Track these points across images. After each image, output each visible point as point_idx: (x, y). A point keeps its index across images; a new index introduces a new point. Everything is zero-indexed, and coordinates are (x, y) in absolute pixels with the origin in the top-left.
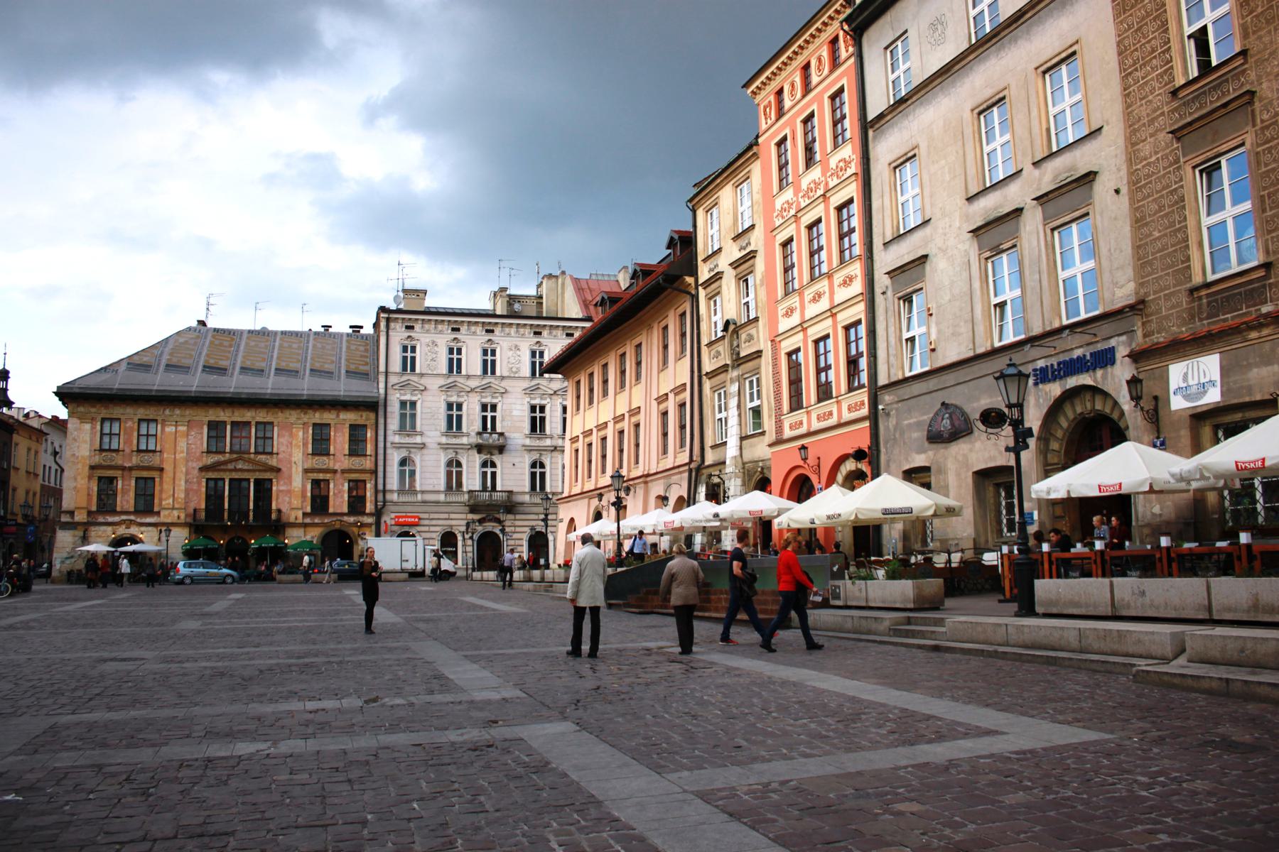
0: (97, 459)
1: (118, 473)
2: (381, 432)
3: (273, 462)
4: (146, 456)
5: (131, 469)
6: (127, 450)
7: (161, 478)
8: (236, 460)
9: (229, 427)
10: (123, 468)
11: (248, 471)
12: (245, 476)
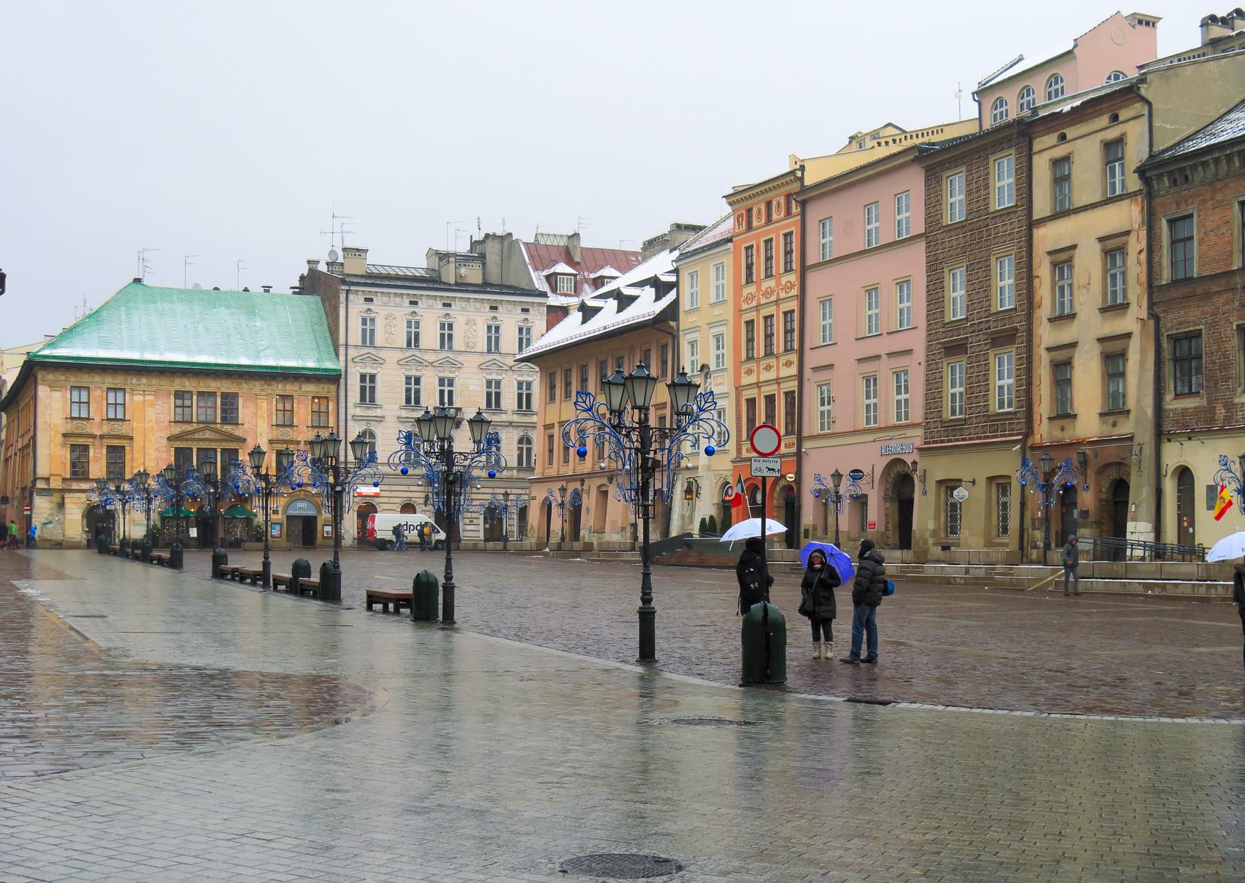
0: (70, 427)
1: (89, 441)
2: (342, 405)
3: (238, 432)
4: (117, 425)
5: (102, 437)
6: (97, 419)
7: (132, 447)
8: (203, 430)
9: (195, 397)
10: (94, 437)
11: (215, 440)
12: (213, 445)
